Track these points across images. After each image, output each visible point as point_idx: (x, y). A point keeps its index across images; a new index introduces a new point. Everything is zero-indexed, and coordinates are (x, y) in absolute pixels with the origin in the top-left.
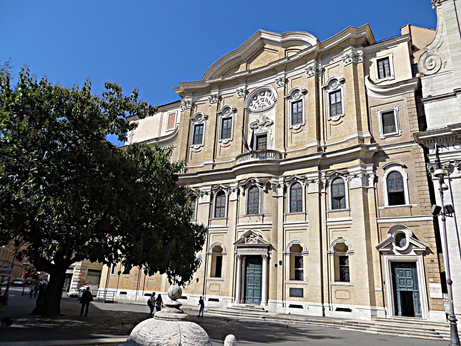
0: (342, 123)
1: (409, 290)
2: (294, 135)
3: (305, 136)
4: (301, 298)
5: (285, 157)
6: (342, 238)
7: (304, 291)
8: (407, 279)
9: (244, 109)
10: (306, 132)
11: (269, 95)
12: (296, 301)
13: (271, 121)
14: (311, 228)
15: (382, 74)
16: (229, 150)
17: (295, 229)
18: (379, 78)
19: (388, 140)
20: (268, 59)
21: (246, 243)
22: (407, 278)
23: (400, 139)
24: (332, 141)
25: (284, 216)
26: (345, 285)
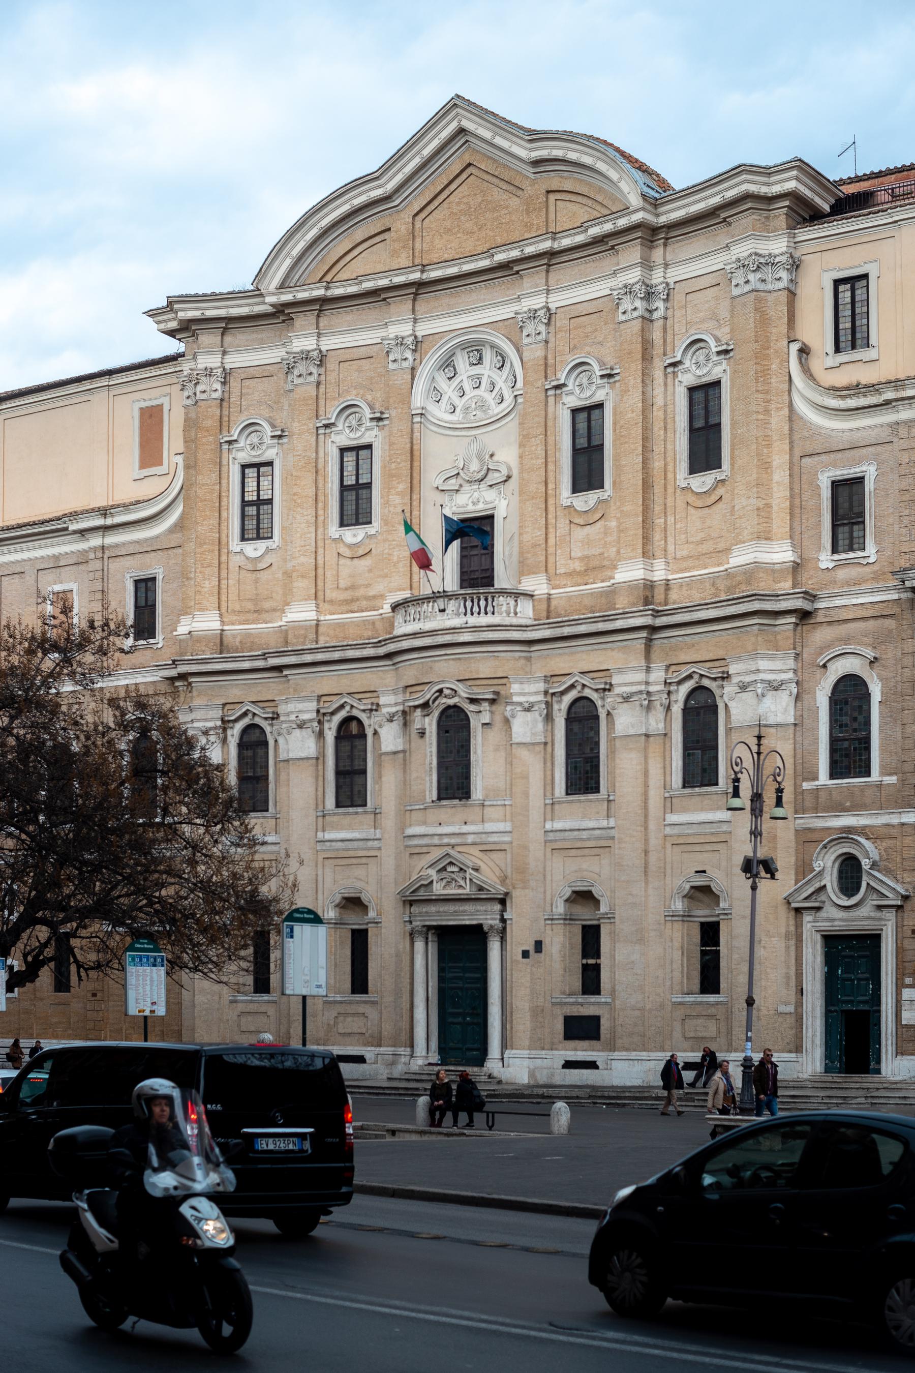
0: (720, 505)
1: (862, 1007)
2: (580, 534)
3: (609, 539)
4: (594, 1042)
6: (704, 872)
7: (602, 1021)
8: (859, 980)
10: (613, 524)
11: (498, 365)
12: (581, 1051)
13: (505, 472)
14: (623, 845)
15: (845, 337)
16: (370, 571)
17: (579, 845)
18: (837, 350)
19: (842, 574)
20: (488, 215)
22: (860, 976)
23: (874, 572)
24: (690, 563)
26: (708, 1003)
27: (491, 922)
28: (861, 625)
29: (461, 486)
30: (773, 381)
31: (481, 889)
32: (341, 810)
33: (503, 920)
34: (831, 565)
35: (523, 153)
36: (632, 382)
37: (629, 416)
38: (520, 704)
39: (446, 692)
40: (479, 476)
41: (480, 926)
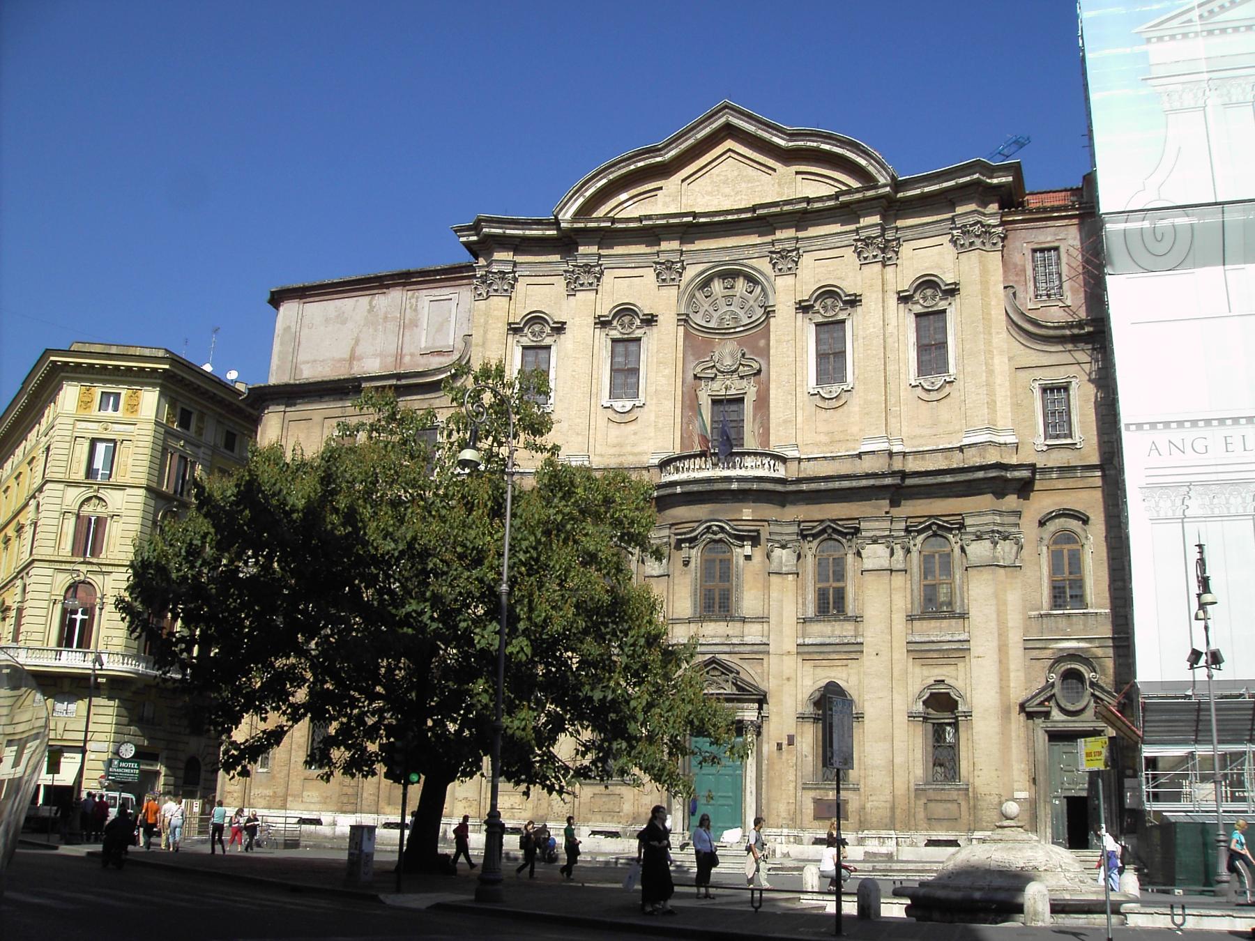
0: (948, 399)
6: (943, 681)
29: (716, 375)
30: (993, 313)
31: (740, 688)
34: (1045, 448)
35: (782, 143)
36: (873, 307)
37: (872, 330)
38: (778, 541)
39: (715, 528)
40: (733, 368)
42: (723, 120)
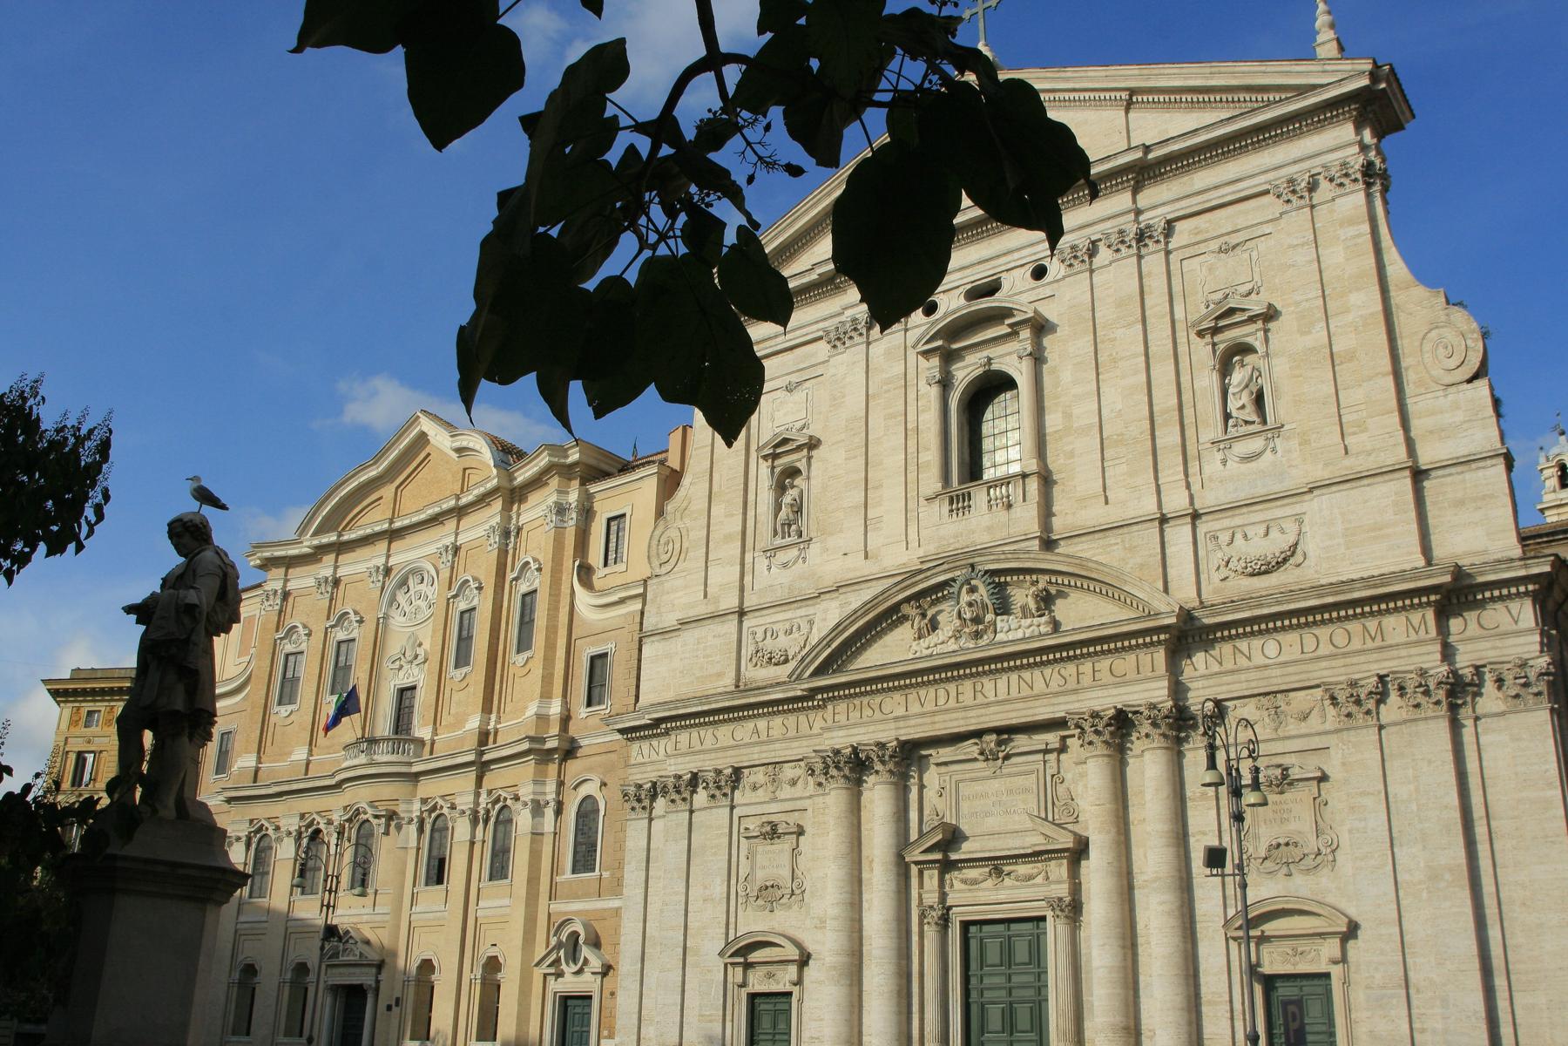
5: (431, 753)
9: (378, 619)
18: (606, 564)
21: (341, 958)
25: (413, 894)
27: (369, 983)
28: (598, 758)
32: (304, 897)
33: (378, 982)
41: (361, 986)
42: (418, 429)
